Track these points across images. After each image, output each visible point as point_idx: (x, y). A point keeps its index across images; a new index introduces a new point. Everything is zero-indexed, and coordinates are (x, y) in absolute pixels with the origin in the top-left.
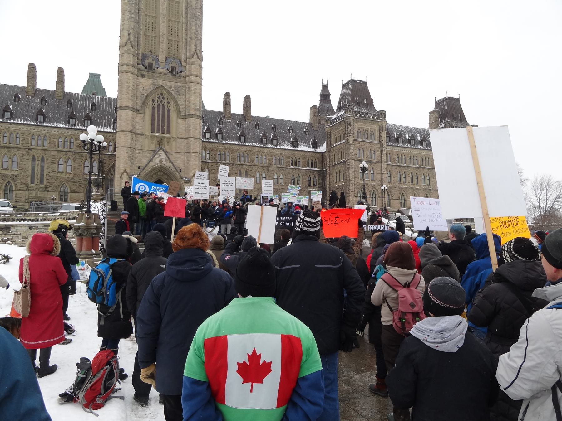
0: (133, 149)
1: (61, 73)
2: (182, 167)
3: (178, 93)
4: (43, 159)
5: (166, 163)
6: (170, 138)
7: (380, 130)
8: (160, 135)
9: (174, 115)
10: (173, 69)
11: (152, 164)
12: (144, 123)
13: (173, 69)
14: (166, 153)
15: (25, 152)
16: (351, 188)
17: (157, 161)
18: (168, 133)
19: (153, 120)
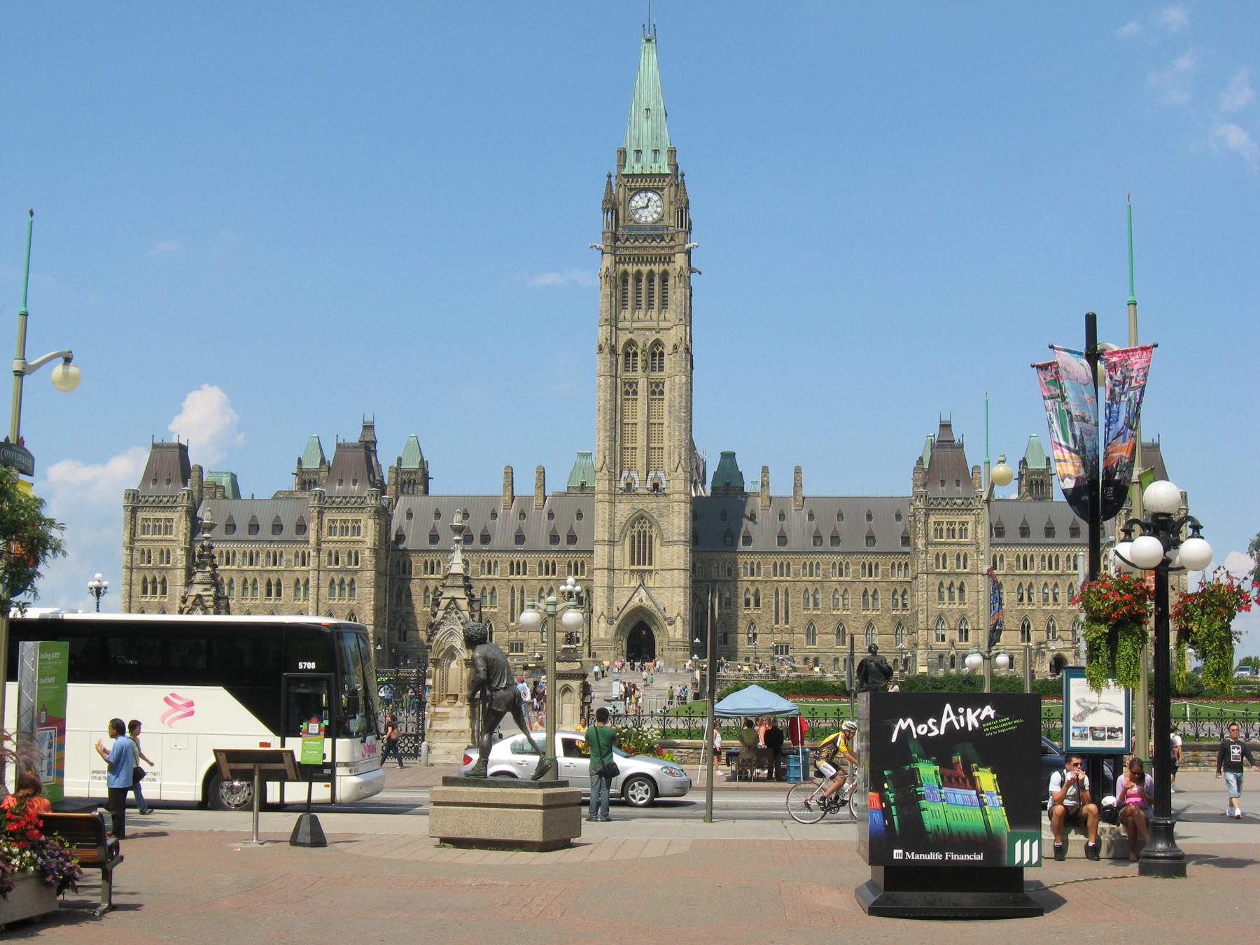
0: (611, 588)
1: (542, 473)
2: (667, 604)
3: (661, 515)
4: (522, 592)
5: (647, 603)
6: (650, 571)
7: (977, 522)
8: (641, 567)
9: (657, 544)
10: (656, 486)
11: (631, 605)
12: (622, 555)
13: (656, 486)
14: (647, 589)
15: (503, 584)
16: (920, 616)
17: (636, 600)
18: (650, 564)
19: (633, 547)
